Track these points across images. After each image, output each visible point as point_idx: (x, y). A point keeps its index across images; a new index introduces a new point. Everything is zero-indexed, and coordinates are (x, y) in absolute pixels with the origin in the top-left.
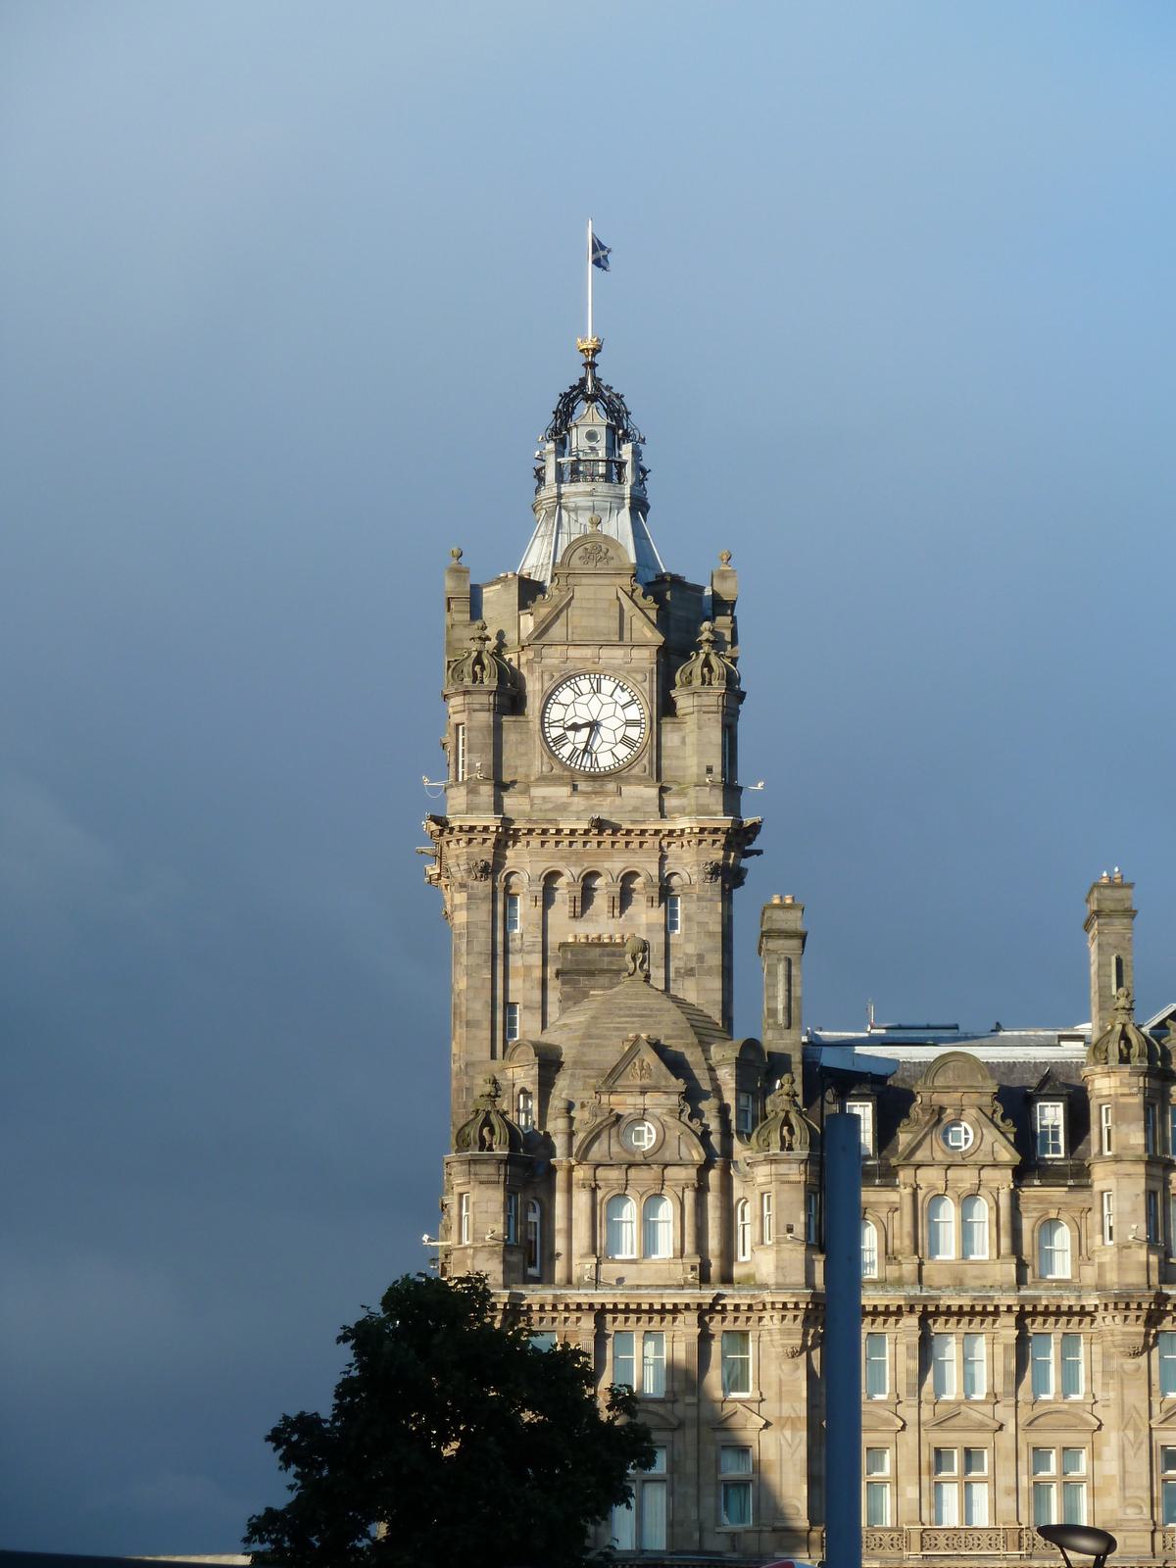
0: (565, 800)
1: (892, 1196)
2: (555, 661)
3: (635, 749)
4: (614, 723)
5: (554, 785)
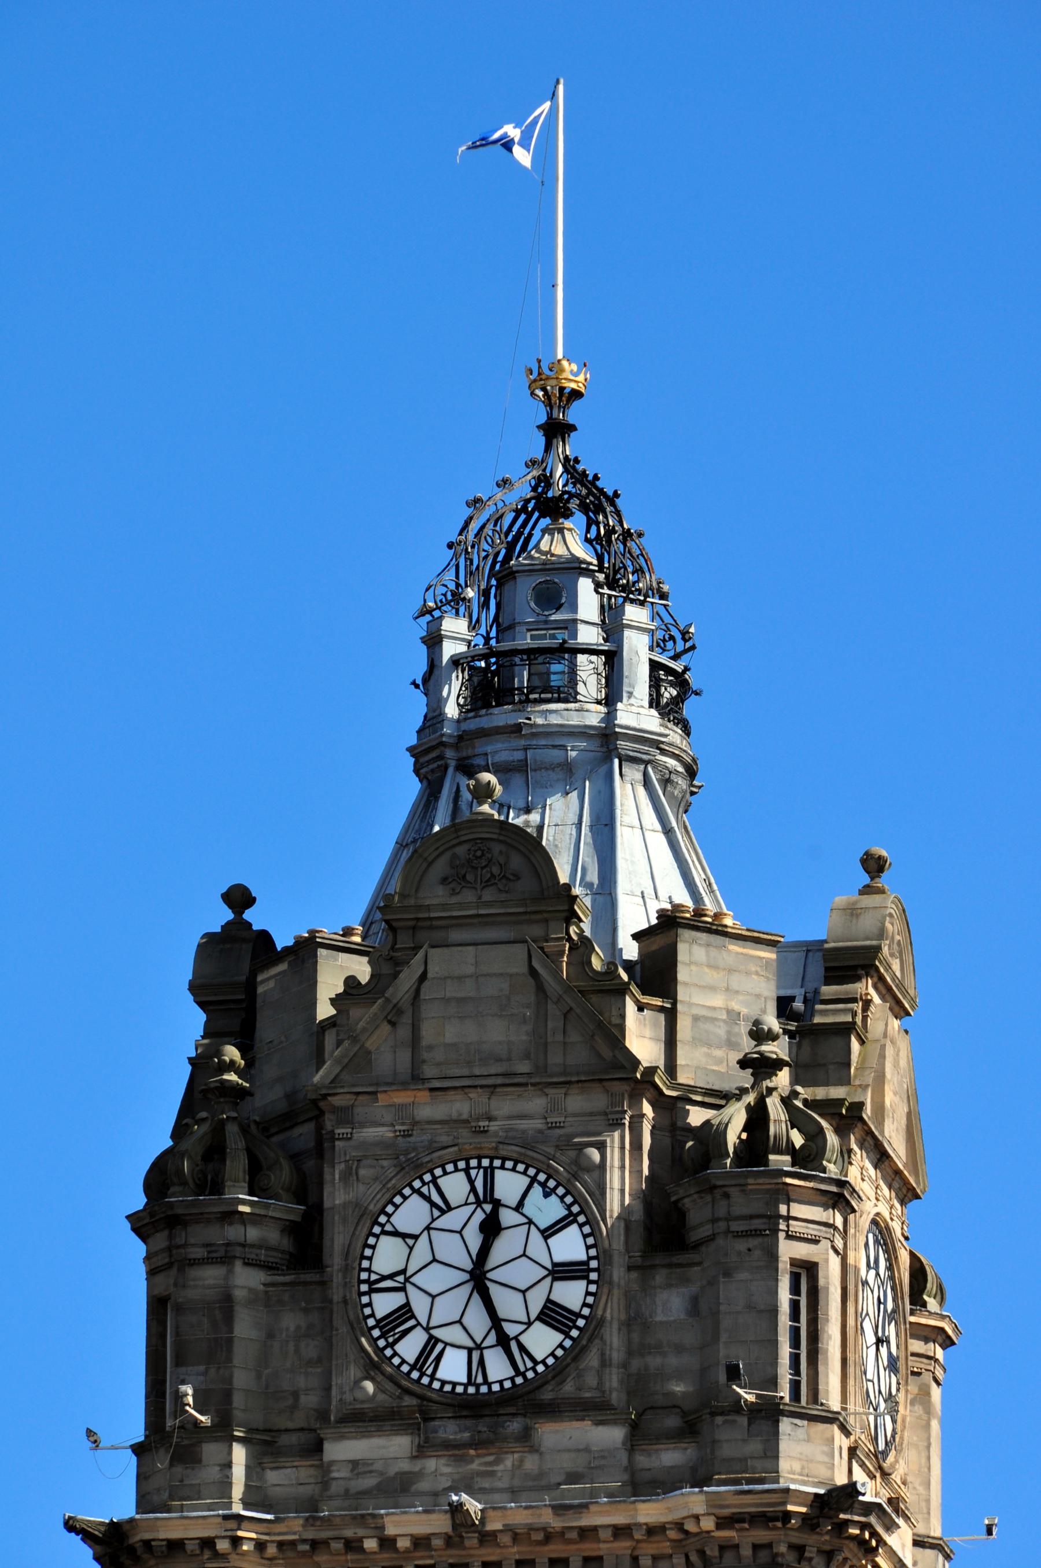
0: (405, 1466)
2: (384, 1132)
3: (575, 1333)
4: (523, 1274)
5: (380, 1432)
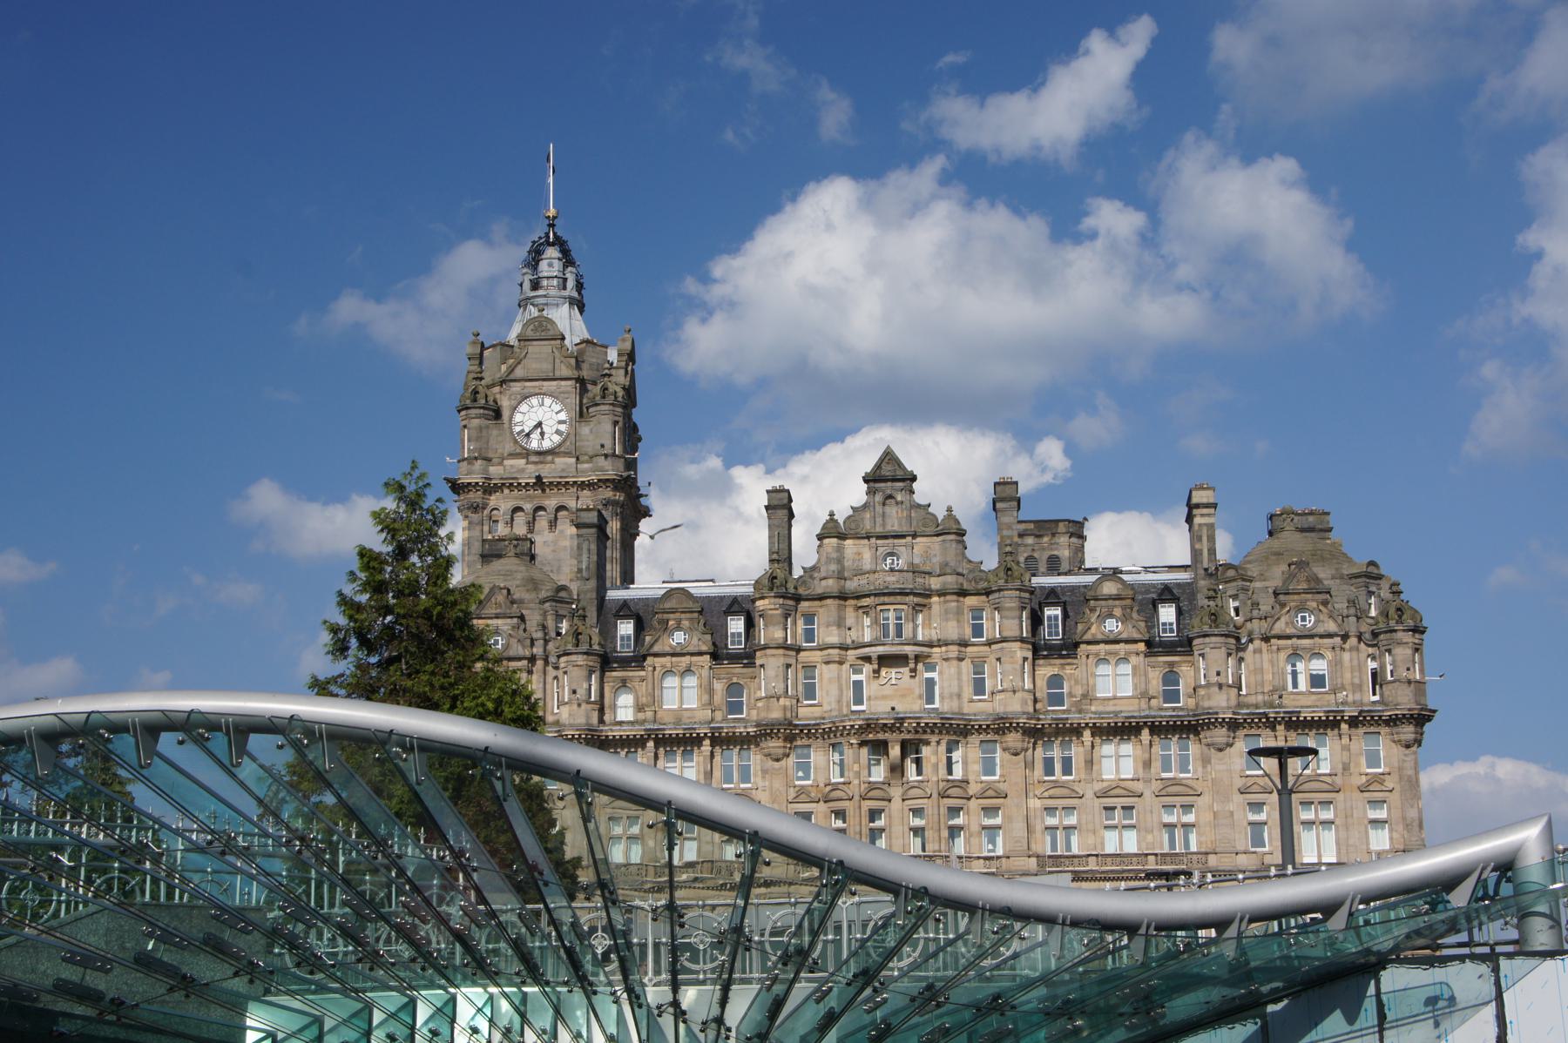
1: (643, 673)
4: (551, 422)
